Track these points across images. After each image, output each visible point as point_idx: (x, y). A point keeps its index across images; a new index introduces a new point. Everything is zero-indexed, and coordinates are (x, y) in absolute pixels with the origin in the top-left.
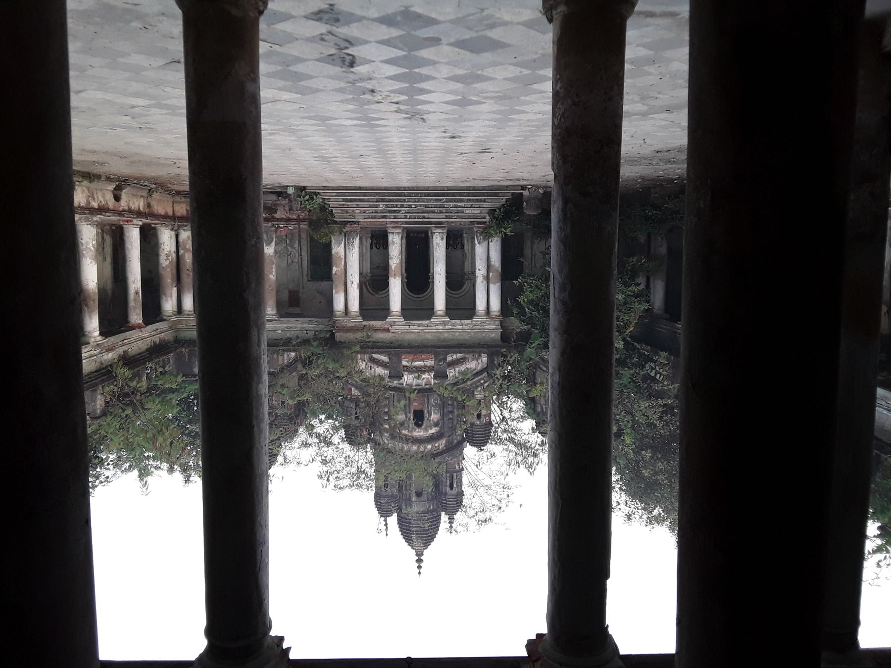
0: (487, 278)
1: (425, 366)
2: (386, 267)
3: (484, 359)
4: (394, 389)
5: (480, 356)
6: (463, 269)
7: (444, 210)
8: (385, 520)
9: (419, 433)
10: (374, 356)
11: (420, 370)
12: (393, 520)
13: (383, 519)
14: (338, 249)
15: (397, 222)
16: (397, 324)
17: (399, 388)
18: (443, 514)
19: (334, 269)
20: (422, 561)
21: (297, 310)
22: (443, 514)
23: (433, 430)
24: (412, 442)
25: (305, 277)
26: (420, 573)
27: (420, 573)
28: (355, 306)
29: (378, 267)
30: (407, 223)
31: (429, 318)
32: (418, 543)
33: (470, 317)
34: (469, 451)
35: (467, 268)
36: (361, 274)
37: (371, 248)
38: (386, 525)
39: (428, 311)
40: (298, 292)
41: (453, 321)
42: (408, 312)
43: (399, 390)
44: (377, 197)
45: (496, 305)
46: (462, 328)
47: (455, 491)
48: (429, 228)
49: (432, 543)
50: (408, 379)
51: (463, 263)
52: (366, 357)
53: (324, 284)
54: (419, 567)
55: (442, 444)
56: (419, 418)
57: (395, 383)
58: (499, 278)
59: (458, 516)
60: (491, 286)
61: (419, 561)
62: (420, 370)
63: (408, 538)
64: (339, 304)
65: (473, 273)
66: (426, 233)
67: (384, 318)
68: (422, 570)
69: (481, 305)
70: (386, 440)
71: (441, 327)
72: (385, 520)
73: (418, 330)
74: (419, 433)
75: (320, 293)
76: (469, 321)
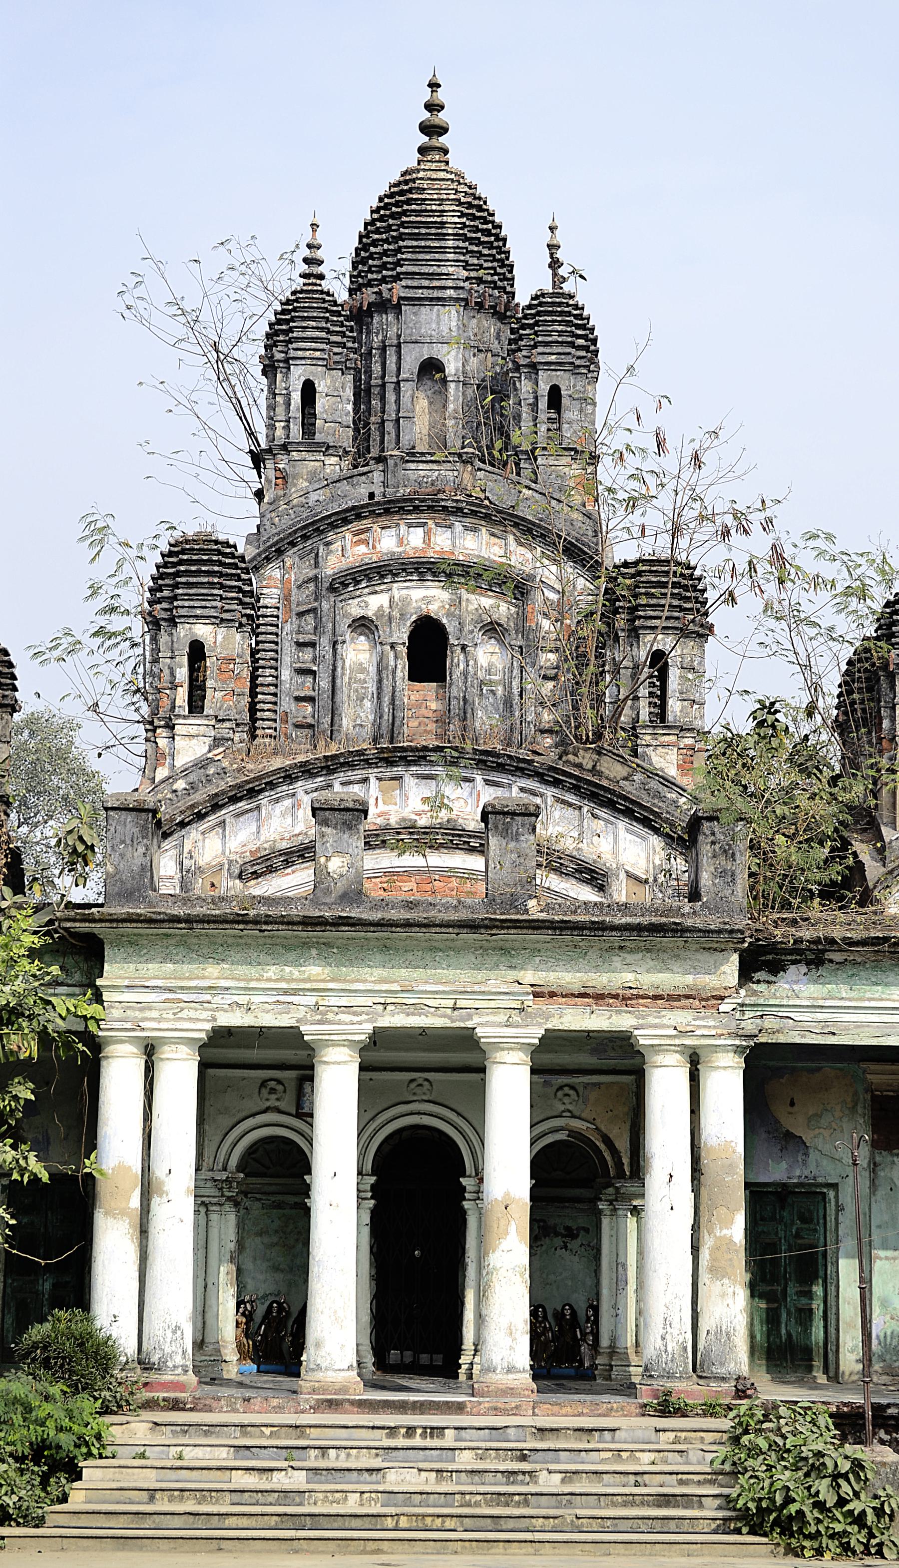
0: (148, 1188)
1: (401, 848)
2: (541, 1232)
3: (167, 866)
4: (520, 768)
5: (184, 885)
6: (240, 1226)
7: (313, 1459)
8: (559, 281)
9: (430, 598)
10: (586, 894)
11: (423, 838)
12: (529, 282)
13: (567, 287)
14: (731, 1308)
15: (496, 1411)
16: (505, 1011)
17: (501, 768)
18: (342, 296)
19: (735, 1229)
20: (427, 129)
21: (879, 1076)
22: (342, 296)
23: (374, 603)
24: (566, 551)
25: (846, 1196)
26: (434, 86)
27: (434, 86)
28: (666, 1087)
29: (571, 1234)
30: (459, 1408)
31: (380, 1039)
32: (436, 190)
33: (221, 1036)
34: (236, 520)
35: (226, 1225)
36: (636, 1211)
37: (596, 1309)
38: (555, 264)
39: (386, 1060)
40: (875, 1145)
41: (285, 1021)
42: (460, 1060)
43: (492, 763)
44: (568, 1513)
45: (120, 1077)
46: (256, 994)
47: (298, 375)
48: (371, 1385)
49: (384, 189)
50: (467, 801)
51: (241, 1244)
52: (620, 892)
53: (777, 1172)
54: (433, 107)
55: (345, 551)
56: (429, 651)
57: (514, 792)
58: (104, 1189)
59: (288, 280)
60: (137, 1167)
61: (431, 129)
62: (423, 838)
63: (476, 210)
64: (726, 1088)
65: (203, 1206)
66: (381, 1364)
67: (552, 1041)
68: (426, 95)
69: (180, 1077)
70: (550, 573)
71: (334, 1001)
72: (559, 281)
73: (425, 995)
74: (430, 598)
75: (790, 1143)
76: (228, 1019)
